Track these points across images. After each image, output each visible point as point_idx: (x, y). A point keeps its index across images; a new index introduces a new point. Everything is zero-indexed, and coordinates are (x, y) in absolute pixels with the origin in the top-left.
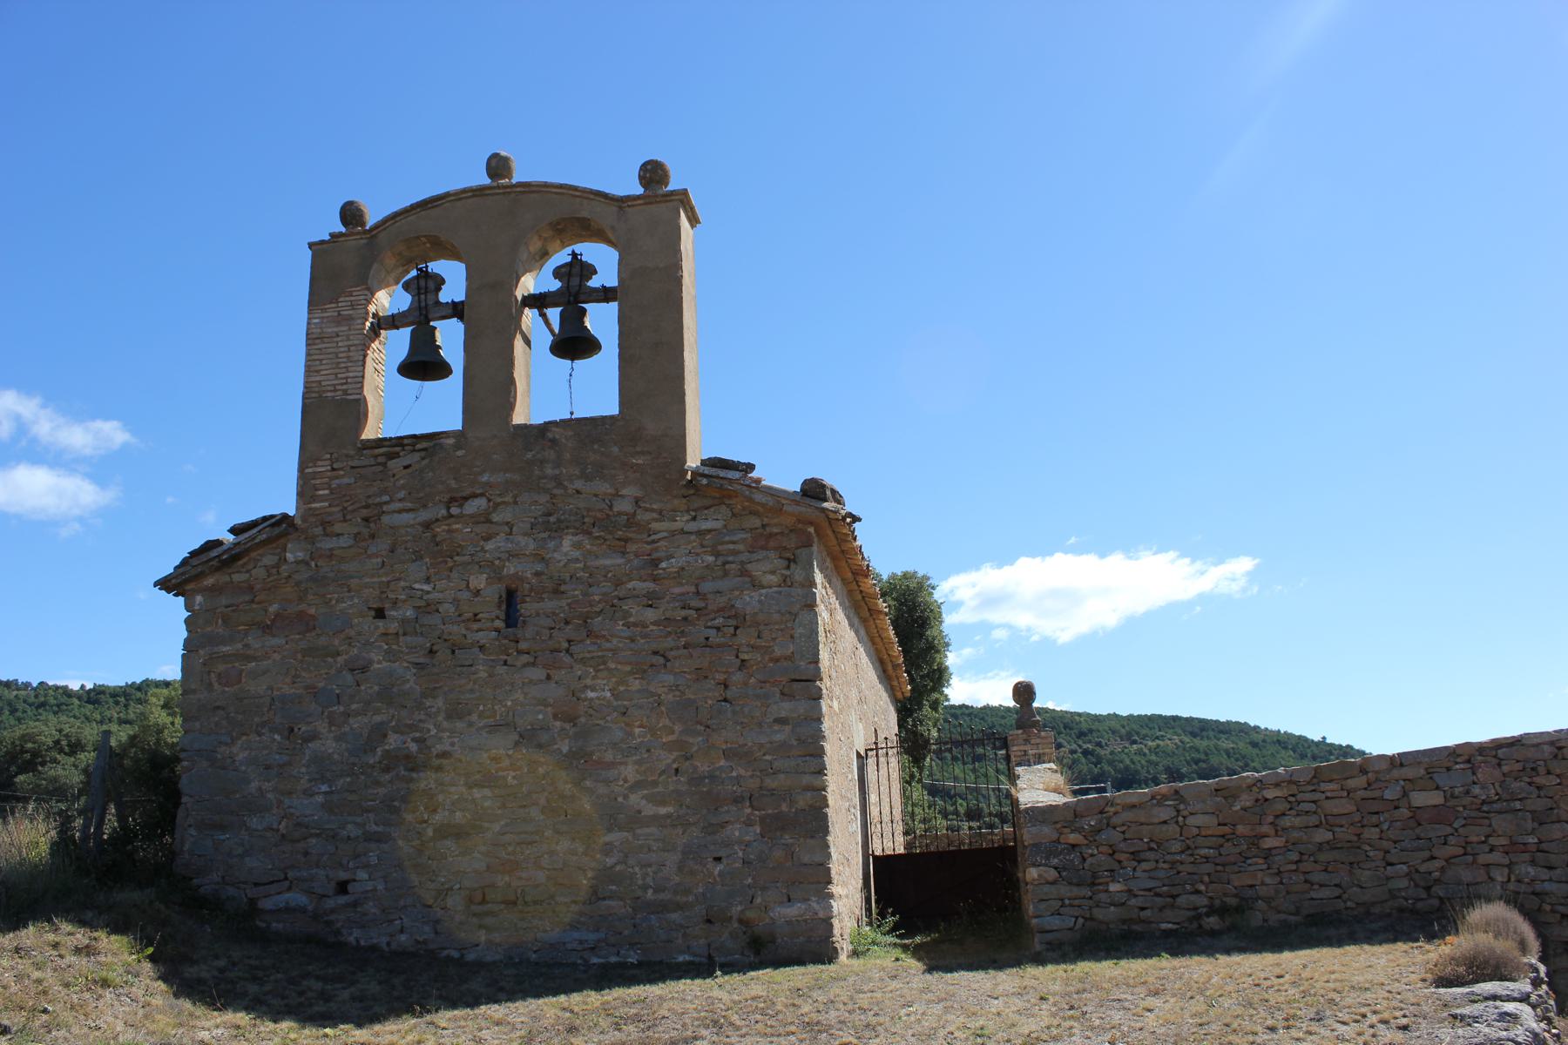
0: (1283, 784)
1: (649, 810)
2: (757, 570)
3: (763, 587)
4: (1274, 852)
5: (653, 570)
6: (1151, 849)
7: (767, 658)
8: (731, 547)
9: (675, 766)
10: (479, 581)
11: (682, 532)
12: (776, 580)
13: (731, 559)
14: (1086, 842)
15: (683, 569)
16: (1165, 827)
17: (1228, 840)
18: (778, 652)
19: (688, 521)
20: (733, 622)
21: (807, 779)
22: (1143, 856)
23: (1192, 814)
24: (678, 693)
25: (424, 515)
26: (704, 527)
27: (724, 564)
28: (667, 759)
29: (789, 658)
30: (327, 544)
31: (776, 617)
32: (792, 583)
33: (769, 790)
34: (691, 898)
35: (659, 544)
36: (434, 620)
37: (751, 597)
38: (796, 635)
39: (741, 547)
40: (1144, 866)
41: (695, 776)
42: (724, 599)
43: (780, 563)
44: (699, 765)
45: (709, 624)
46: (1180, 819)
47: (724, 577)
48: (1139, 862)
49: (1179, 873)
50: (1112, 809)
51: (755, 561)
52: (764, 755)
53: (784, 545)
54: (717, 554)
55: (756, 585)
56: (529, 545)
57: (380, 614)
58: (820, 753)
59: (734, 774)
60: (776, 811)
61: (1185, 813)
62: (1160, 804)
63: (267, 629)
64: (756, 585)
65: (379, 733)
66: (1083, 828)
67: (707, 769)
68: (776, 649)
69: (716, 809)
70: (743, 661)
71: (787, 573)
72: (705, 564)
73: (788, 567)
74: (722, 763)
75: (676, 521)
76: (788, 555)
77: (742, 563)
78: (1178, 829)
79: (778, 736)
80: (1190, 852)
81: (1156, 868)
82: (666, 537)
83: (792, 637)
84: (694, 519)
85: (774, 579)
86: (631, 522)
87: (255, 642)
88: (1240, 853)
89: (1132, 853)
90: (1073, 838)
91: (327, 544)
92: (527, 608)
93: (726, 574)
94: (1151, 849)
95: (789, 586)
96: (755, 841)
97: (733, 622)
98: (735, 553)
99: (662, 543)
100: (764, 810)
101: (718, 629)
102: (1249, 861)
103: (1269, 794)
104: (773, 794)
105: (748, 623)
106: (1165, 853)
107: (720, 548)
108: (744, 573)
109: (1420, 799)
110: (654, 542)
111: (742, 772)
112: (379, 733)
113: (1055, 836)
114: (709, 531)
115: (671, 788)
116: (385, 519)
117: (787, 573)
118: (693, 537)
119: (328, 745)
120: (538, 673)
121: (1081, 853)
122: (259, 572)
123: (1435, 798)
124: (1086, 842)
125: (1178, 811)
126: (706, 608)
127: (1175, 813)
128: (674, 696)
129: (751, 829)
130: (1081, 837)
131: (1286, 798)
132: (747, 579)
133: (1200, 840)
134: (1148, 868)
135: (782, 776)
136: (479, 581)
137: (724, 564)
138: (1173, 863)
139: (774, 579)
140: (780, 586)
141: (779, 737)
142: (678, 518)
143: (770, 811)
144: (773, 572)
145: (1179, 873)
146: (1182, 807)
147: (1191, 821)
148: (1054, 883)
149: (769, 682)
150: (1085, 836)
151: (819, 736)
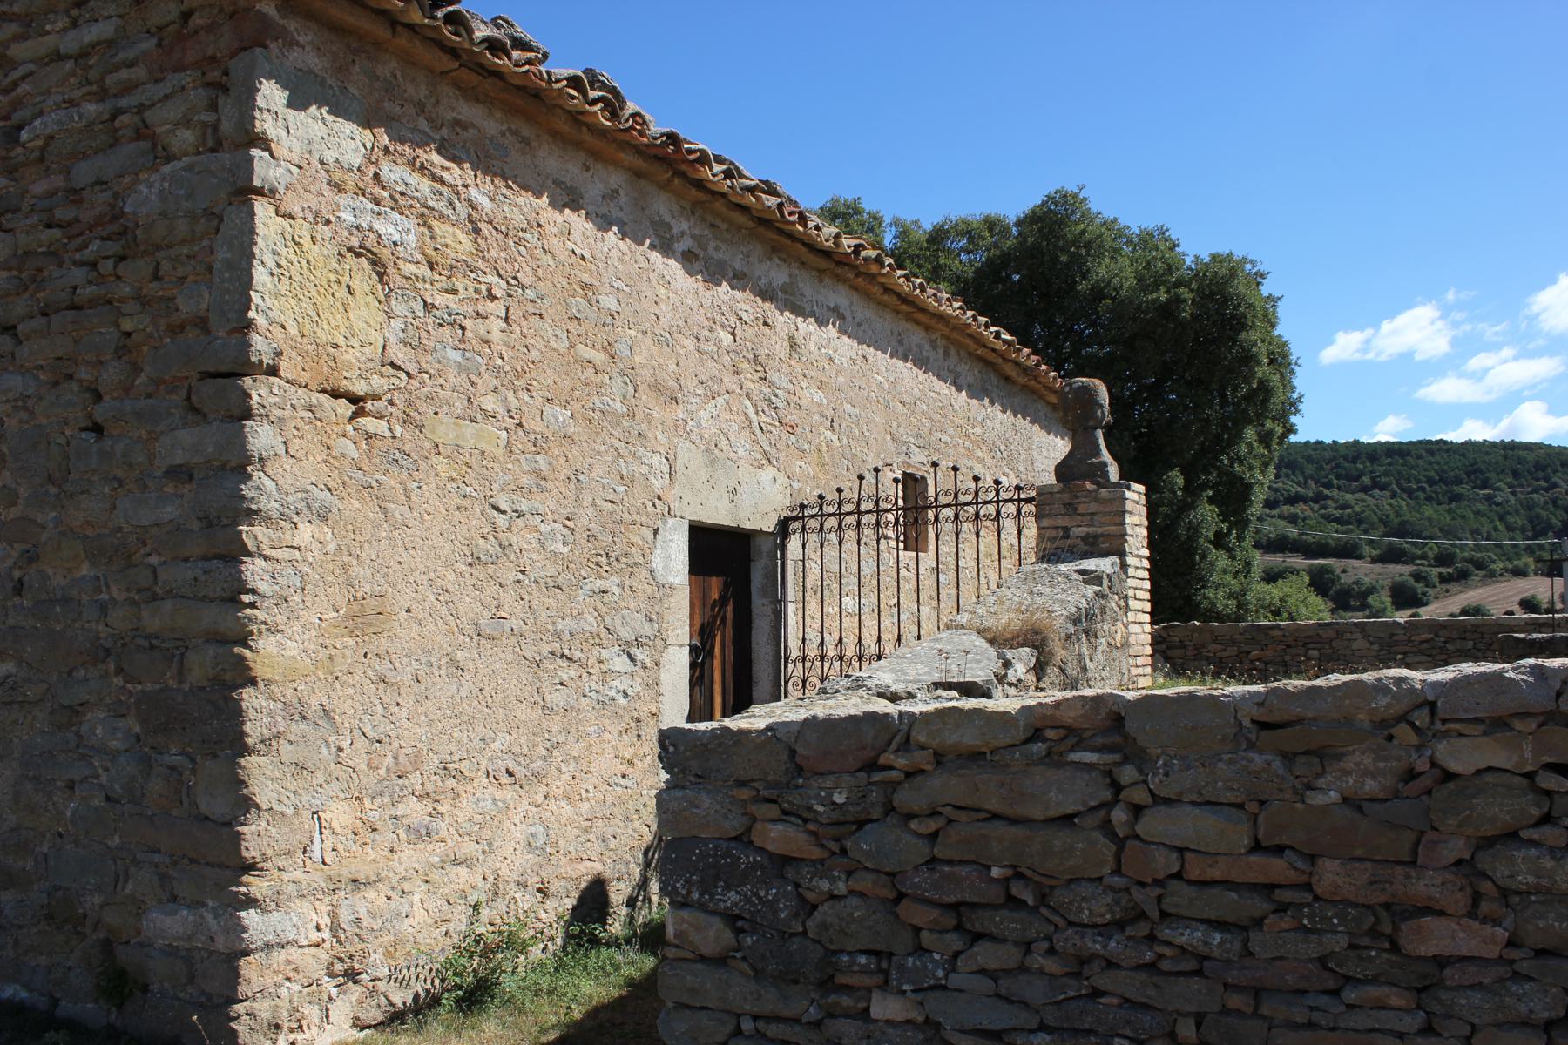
0: (1518, 725)
2: (163, 118)
3: (169, 158)
4: (1452, 975)
5: (8, 151)
6: (1013, 902)
7: (162, 322)
8: (124, 74)
9: (17, 574)
11: (58, 57)
12: (192, 139)
13: (123, 103)
14: (816, 853)
15: (51, 137)
16: (1060, 838)
17: (1281, 909)
18: (186, 306)
19: (64, 30)
20: (113, 248)
21: (210, 616)
22: (979, 922)
23: (1158, 800)
24: (24, 415)
26: (87, 39)
27: (113, 117)
29: (202, 324)
31: (182, 227)
32: (221, 144)
33: (148, 637)
34: (29, 864)
35: (19, 90)
37: (151, 186)
38: (217, 266)
39: (140, 73)
40: (986, 955)
41: (44, 597)
42: (106, 196)
43: (198, 96)
44: (50, 572)
45: (77, 256)
46: (1119, 815)
47: (111, 146)
48: (977, 937)
49: (1096, 993)
50: (901, 762)
51: (160, 101)
52: (150, 555)
53: (210, 53)
54: (102, 95)
55: (162, 154)
59: (105, 596)
60: (157, 687)
61: (1139, 796)
62: (1053, 759)
64: (162, 154)
66: (810, 809)
67: (63, 582)
68: (180, 301)
69: (70, 673)
70: (129, 334)
71: (209, 117)
72: (84, 122)
73: (213, 107)
74: (85, 570)
75: (48, 33)
76: (214, 75)
77: (141, 108)
78: (1107, 849)
79: (169, 509)
80: (1142, 929)
81: (1023, 969)
82: (31, 73)
83: (210, 269)
84: (75, 24)
85: (187, 136)
88: (1322, 961)
89: (955, 907)
90: (778, 836)
93: (114, 142)
94: (1013, 902)
95: (213, 150)
96: (127, 751)
97: (113, 248)
98: (128, 88)
99: (25, 87)
100: (140, 683)
101: (93, 265)
102: (1350, 995)
103: (1462, 756)
104: (152, 647)
105: (142, 248)
106: (1061, 923)
107: (110, 80)
108: (143, 132)
110: (15, 84)
111: (115, 592)
113: (733, 825)
114: (93, 46)
115: (11, 622)
117: (209, 117)
118: (69, 65)
121: (797, 885)
124: (816, 853)
125: (1117, 787)
126: (77, 220)
127: (1106, 795)
128: (21, 422)
129: (122, 723)
130: (803, 837)
131: (1530, 776)
132: (144, 145)
133: (1180, 898)
134: (992, 965)
135: (168, 605)
137: (113, 117)
138: (1084, 961)
139: (187, 136)
140: (199, 153)
141: (169, 512)
142: (48, 27)
143: (149, 686)
144: (186, 122)
145: (1096, 993)
146: (1128, 774)
147: (1154, 824)
148: (720, 961)
149: (165, 382)
150: (814, 833)
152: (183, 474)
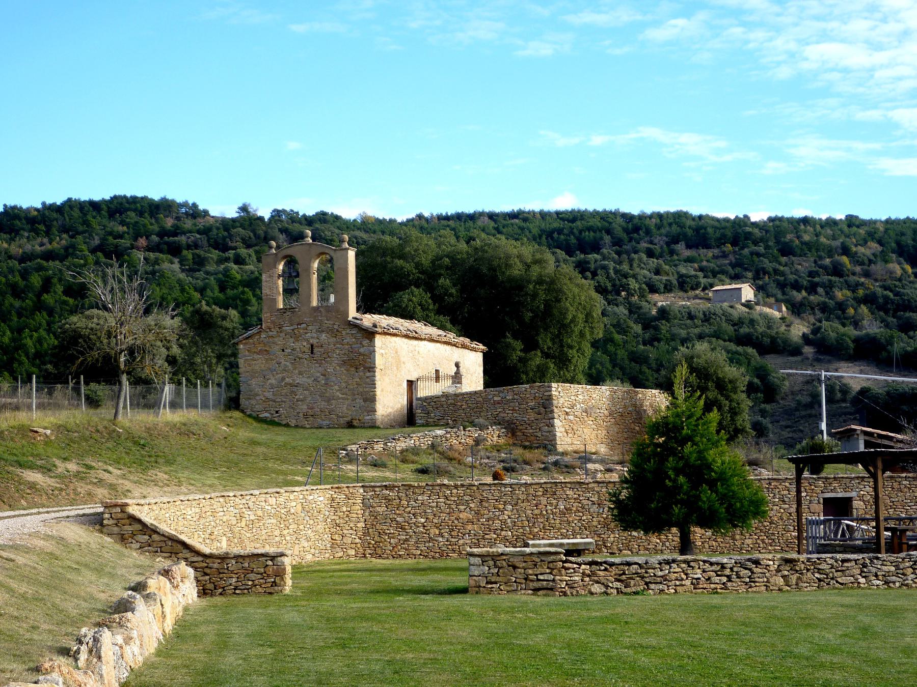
1: (341, 396)
10: (305, 344)
25: (292, 328)
28: (344, 385)
30: (271, 333)
36: (295, 352)
56: (315, 335)
57: (283, 351)
58: (375, 384)
63: (258, 353)
64: (363, 346)
65: (283, 379)
86: (337, 331)
87: (256, 356)
90: (425, 404)
91: (271, 333)
92: (315, 350)
109: (496, 399)
112: (283, 379)
116: (284, 328)
119: (273, 381)
120: (317, 365)
122: (255, 340)
123: (500, 398)
136: (305, 344)
151: (374, 381)
152: (368, 377)
